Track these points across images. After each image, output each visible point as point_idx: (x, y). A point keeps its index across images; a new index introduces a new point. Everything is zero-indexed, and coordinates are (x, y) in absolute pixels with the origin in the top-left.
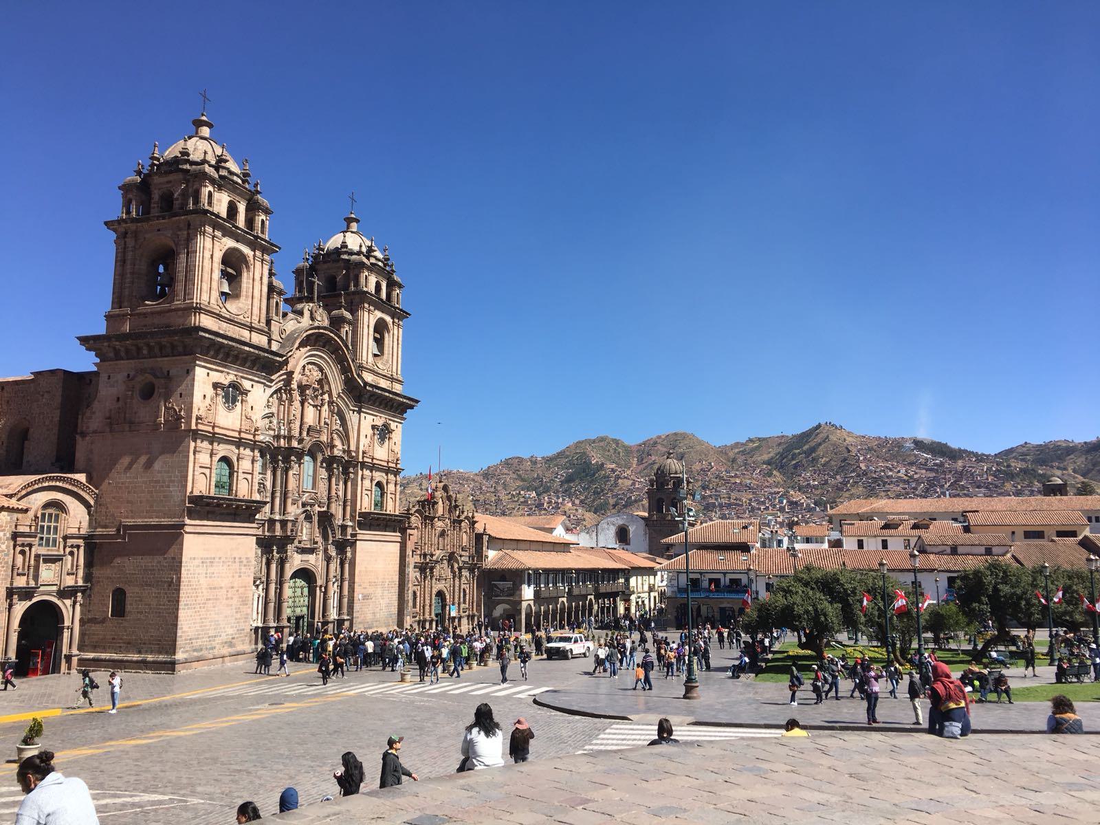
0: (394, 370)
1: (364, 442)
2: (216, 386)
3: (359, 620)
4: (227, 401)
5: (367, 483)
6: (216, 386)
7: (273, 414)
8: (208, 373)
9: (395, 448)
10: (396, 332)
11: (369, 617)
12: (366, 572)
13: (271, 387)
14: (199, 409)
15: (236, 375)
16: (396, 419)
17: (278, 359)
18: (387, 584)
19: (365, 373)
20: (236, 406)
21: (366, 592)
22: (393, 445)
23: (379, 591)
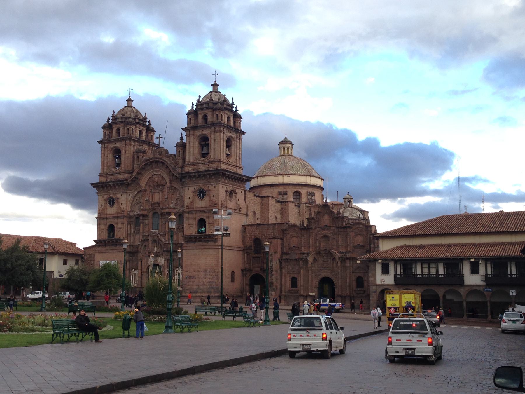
0: (212, 157)
1: (187, 202)
2: (105, 200)
3: (187, 288)
4: (110, 204)
5: (191, 221)
6: (105, 200)
7: (140, 202)
8: (103, 197)
9: (214, 199)
10: (212, 137)
11: (194, 287)
12: (191, 265)
13: (132, 192)
14: (100, 210)
15: (113, 194)
16: (212, 183)
17: (124, 182)
18: (208, 271)
19: (186, 168)
20: (114, 205)
21: (190, 275)
22: (212, 197)
23: (202, 275)
